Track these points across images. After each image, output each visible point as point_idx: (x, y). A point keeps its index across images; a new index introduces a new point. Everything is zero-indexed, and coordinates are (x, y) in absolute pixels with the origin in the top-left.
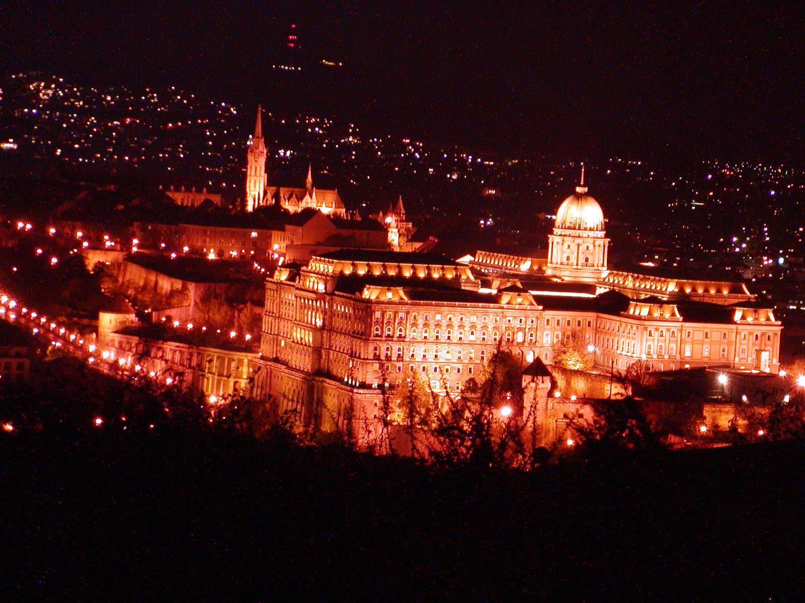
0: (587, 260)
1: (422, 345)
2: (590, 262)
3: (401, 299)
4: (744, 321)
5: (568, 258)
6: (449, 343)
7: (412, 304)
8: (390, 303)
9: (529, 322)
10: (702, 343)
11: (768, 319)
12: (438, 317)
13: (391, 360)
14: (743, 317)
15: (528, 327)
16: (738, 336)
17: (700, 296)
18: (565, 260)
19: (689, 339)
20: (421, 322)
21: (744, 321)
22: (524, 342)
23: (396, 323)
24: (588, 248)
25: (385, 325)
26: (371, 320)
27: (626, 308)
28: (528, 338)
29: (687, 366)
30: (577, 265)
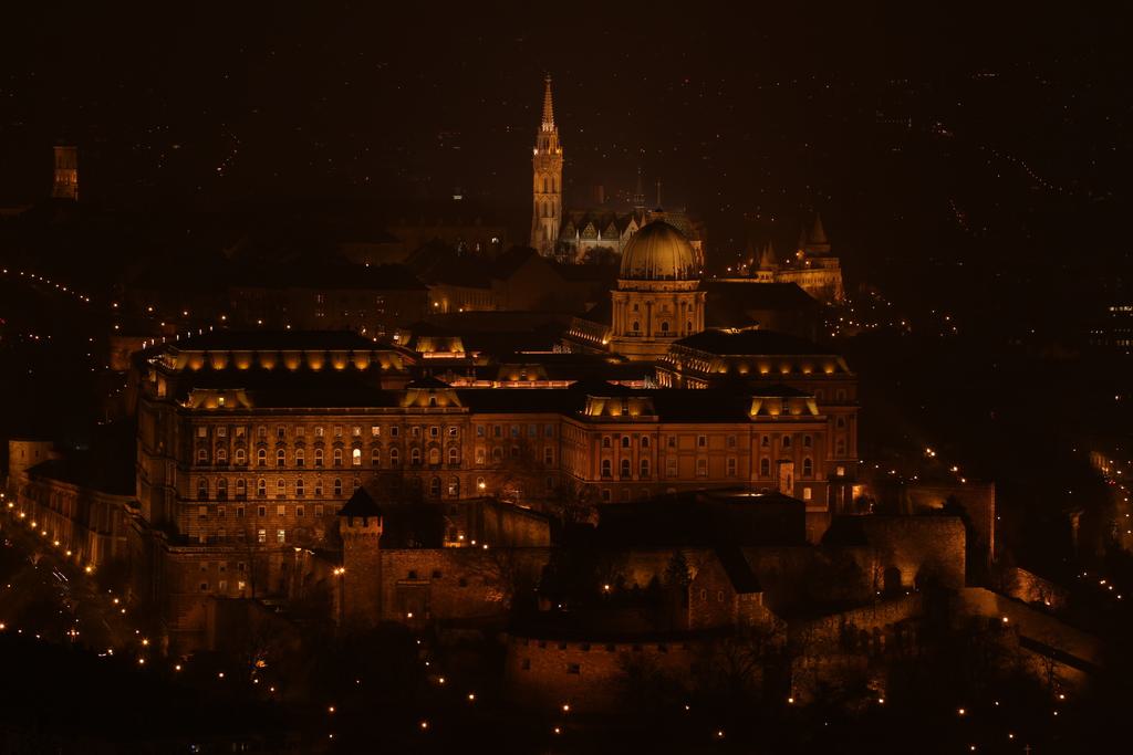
0: (665, 326)
1: (276, 475)
3: (242, 406)
5: (636, 326)
6: (320, 471)
12: (300, 431)
13: (227, 500)
16: (754, 441)
18: (631, 329)
19: (671, 449)
20: (272, 440)
22: (441, 463)
23: (232, 444)
25: (214, 447)
26: (192, 442)
30: (649, 335)
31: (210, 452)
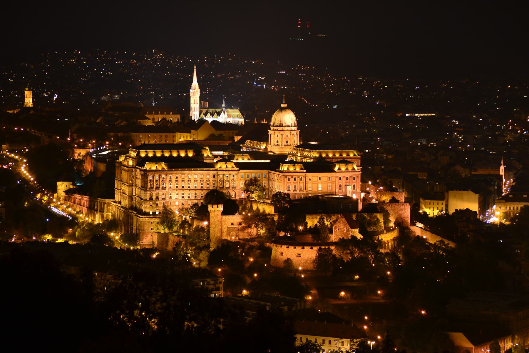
0: (287, 142)
1: (175, 191)
2: (289, 143)
3: (163, 168)
4: (339, 171)
5: (278, 142)
7: (168, 171)
8: (157, 170)
9: (232, 177)
10: (318, 183)
11: (354, 169)
12: (183, 176)
14: (339, 169)
15: (231, 179)
17: (330, 158)
18: (276, 143)
19: (310, 181)
20: (174, 179)
21: (339, 171)
24: (287, 136)
27: (279, 168)
28: (232, 185)
29: (310, 195)
31: (153, 184)
